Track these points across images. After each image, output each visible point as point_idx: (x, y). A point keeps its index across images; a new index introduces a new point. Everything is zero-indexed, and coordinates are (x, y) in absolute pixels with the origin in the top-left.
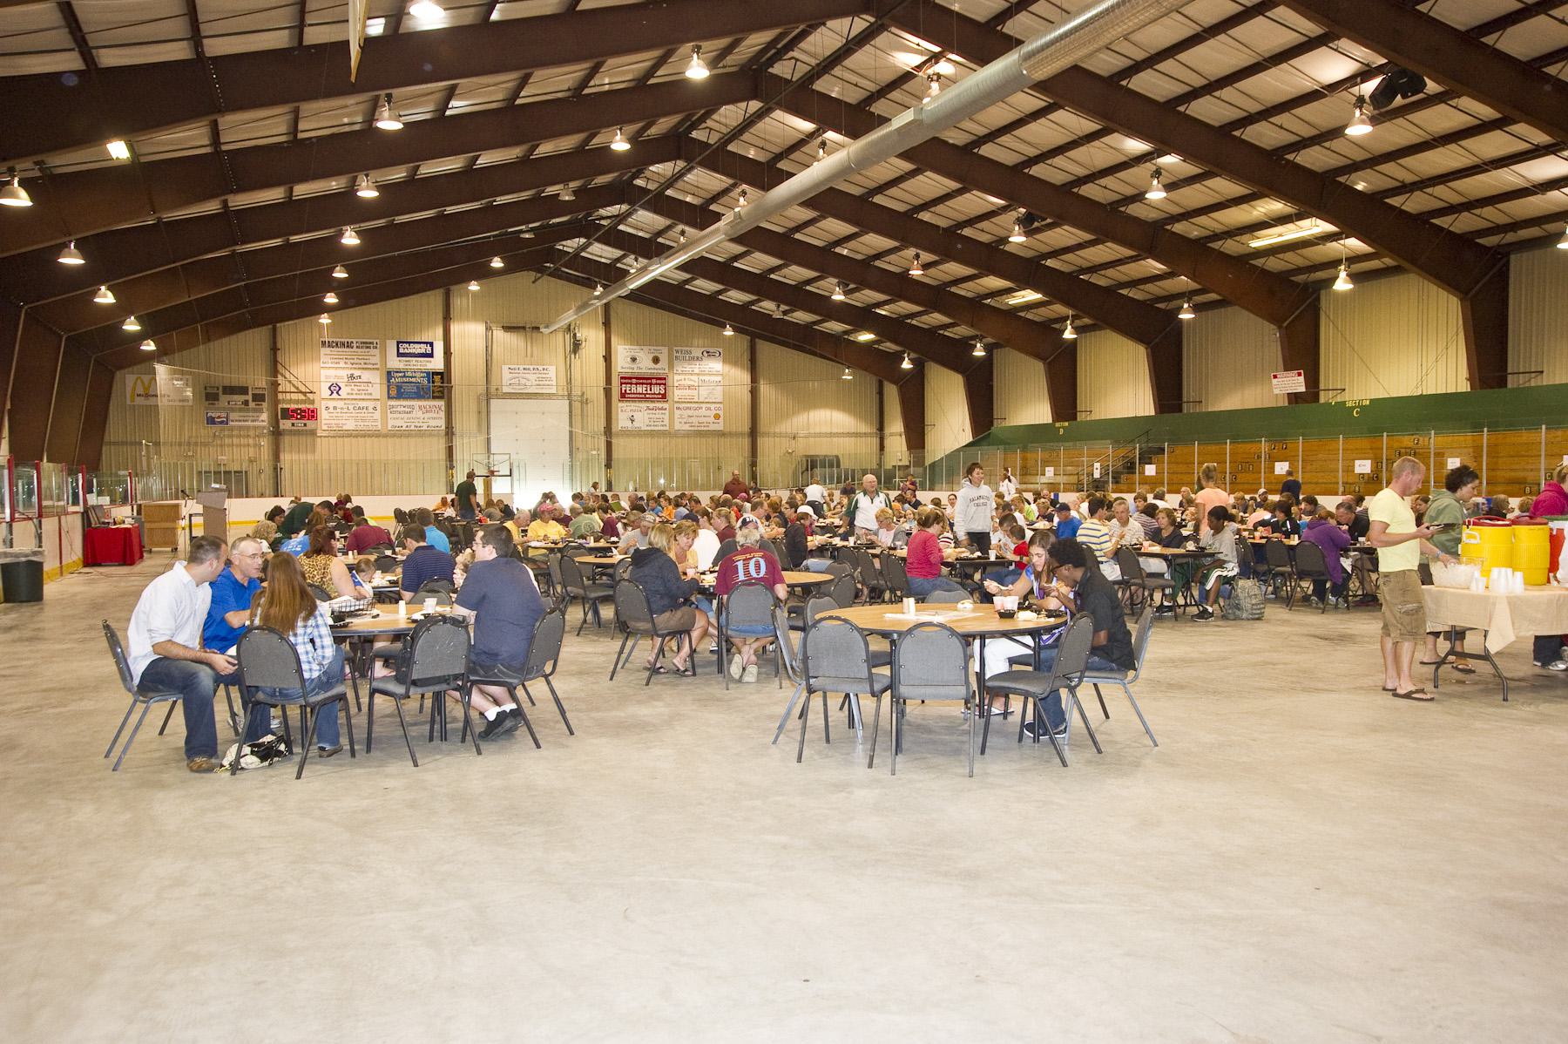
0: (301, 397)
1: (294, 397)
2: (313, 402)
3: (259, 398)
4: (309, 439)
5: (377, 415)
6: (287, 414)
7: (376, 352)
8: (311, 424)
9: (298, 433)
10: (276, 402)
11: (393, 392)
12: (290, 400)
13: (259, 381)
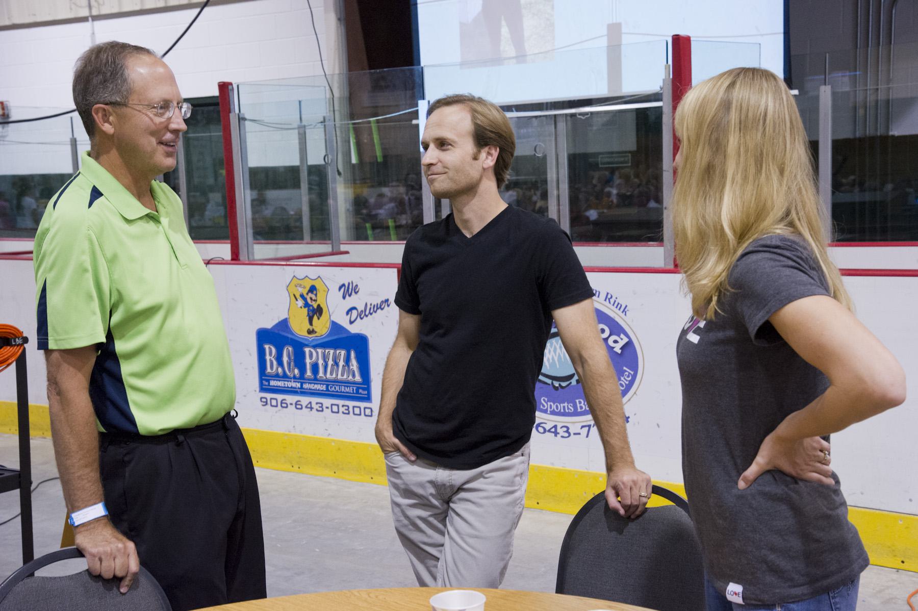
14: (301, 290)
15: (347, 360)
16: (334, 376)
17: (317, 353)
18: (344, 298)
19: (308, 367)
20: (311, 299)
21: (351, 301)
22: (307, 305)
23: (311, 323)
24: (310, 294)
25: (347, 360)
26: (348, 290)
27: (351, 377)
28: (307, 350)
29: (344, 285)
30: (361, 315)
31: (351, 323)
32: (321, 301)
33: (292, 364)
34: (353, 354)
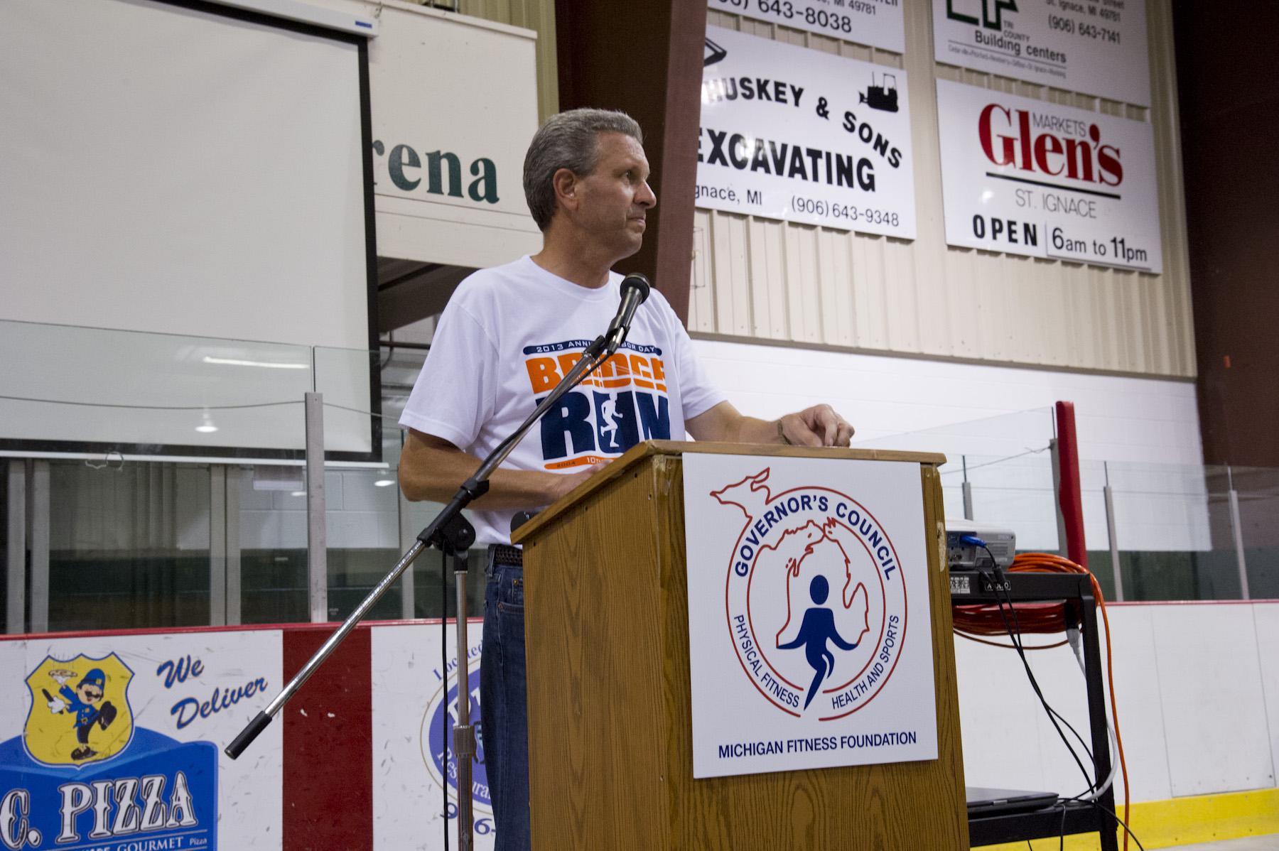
14: (62, 680)
15: (167, 793)
16: (132, 825)
17: (94, 792)
18: (168, 684)
19: (67, 820)
20: (89, 694)
21: (180, 691)
22: (75, 705)
23: (83, 737)
24: (86, 687)
25: (167, 793)
26: (175, 672)
27: (172, 821)
28: (68, 790)
29: (170, 663)
30: (202, 712)
31: (181, 725)
32: (112, 693)
33: (24, 823)
34: (180, 779)
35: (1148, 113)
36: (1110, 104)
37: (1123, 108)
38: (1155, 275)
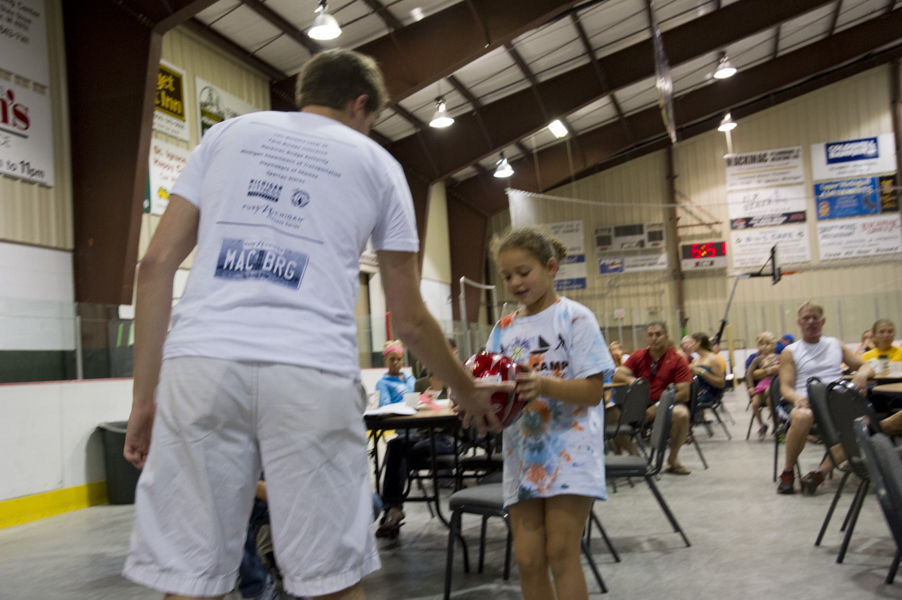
0: (705, 230)
1: (698, 231)
2: (719, 235)
3: (655, 236)
4: (719, 281)
5: (805, 242)
6: (693, 251)
7: (799, 162)
8: (719, 261)
9: (703, 274)
10: (677, 239)
11: (825, 210)
12: (692, 232)
13: (655, 217)
35: (47, 91)
36: (22, 81)
37: (31, 84)
38: (49, 188)
